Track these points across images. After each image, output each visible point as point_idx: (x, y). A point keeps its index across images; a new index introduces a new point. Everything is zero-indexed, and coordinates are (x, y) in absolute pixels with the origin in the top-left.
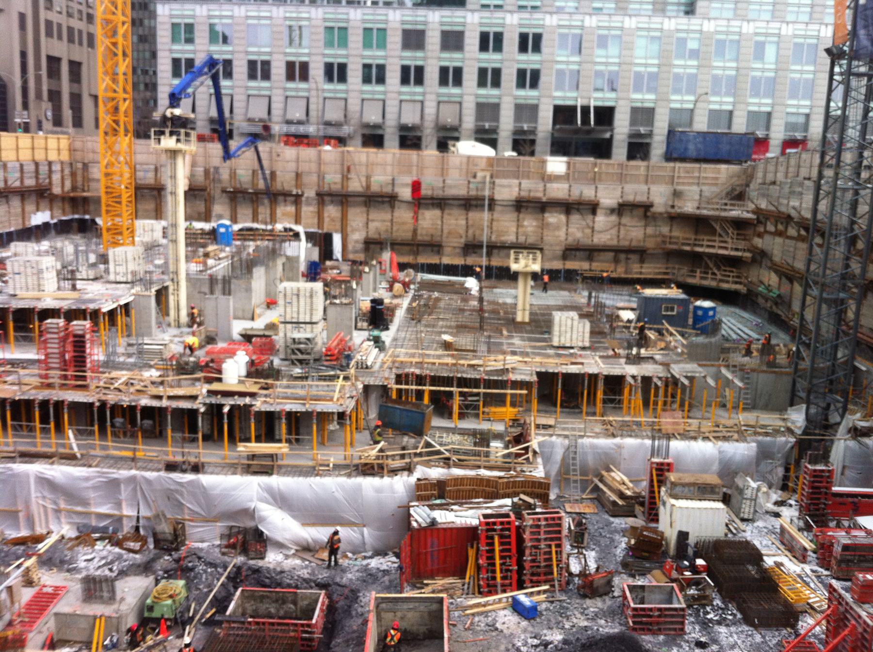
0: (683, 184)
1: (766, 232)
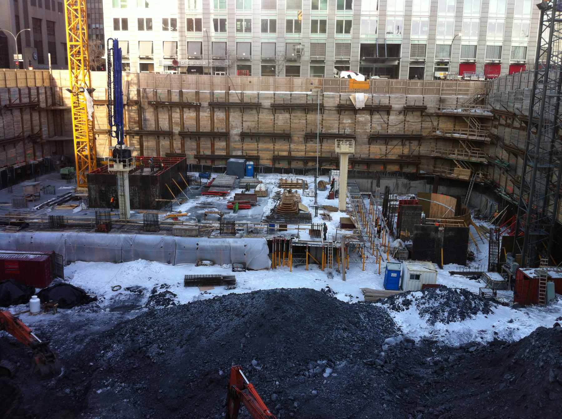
0: (446, 94)
1: (500, 125)
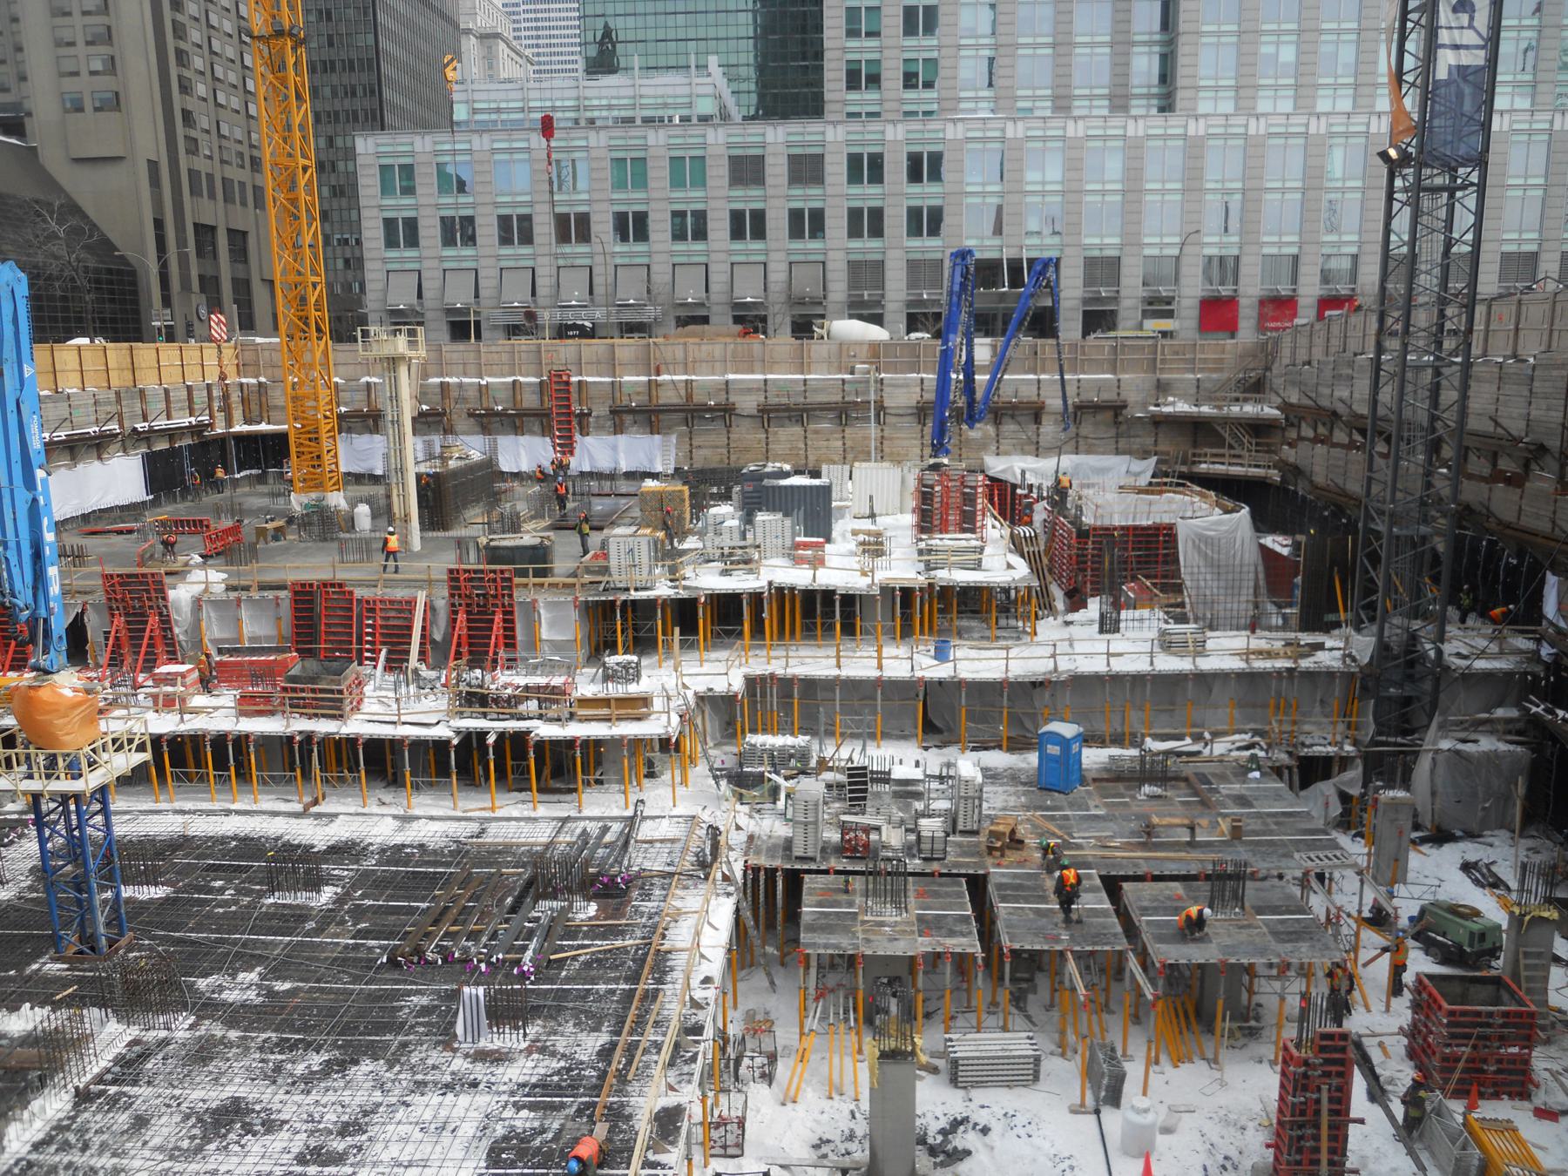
0: (1171, 370)
1: (1301, 438)
